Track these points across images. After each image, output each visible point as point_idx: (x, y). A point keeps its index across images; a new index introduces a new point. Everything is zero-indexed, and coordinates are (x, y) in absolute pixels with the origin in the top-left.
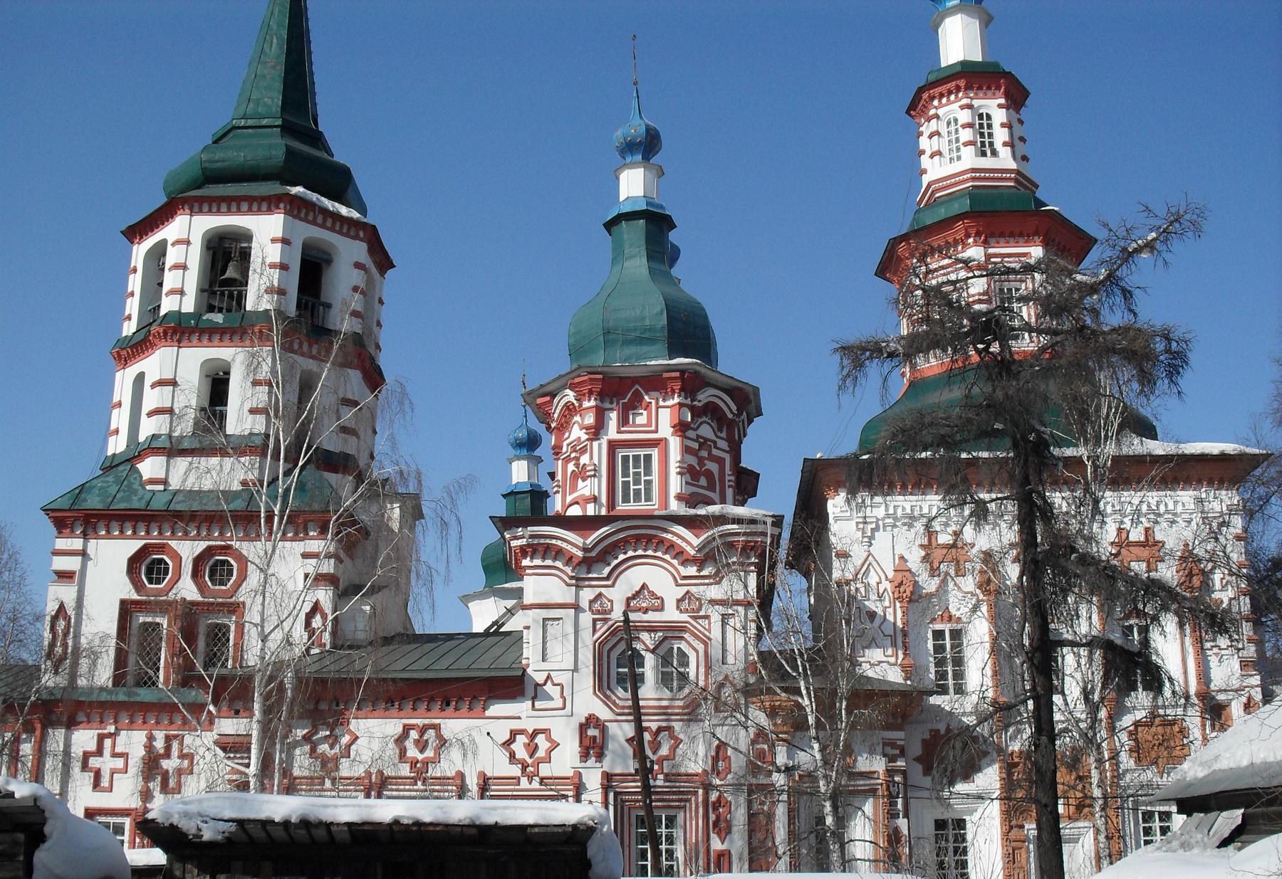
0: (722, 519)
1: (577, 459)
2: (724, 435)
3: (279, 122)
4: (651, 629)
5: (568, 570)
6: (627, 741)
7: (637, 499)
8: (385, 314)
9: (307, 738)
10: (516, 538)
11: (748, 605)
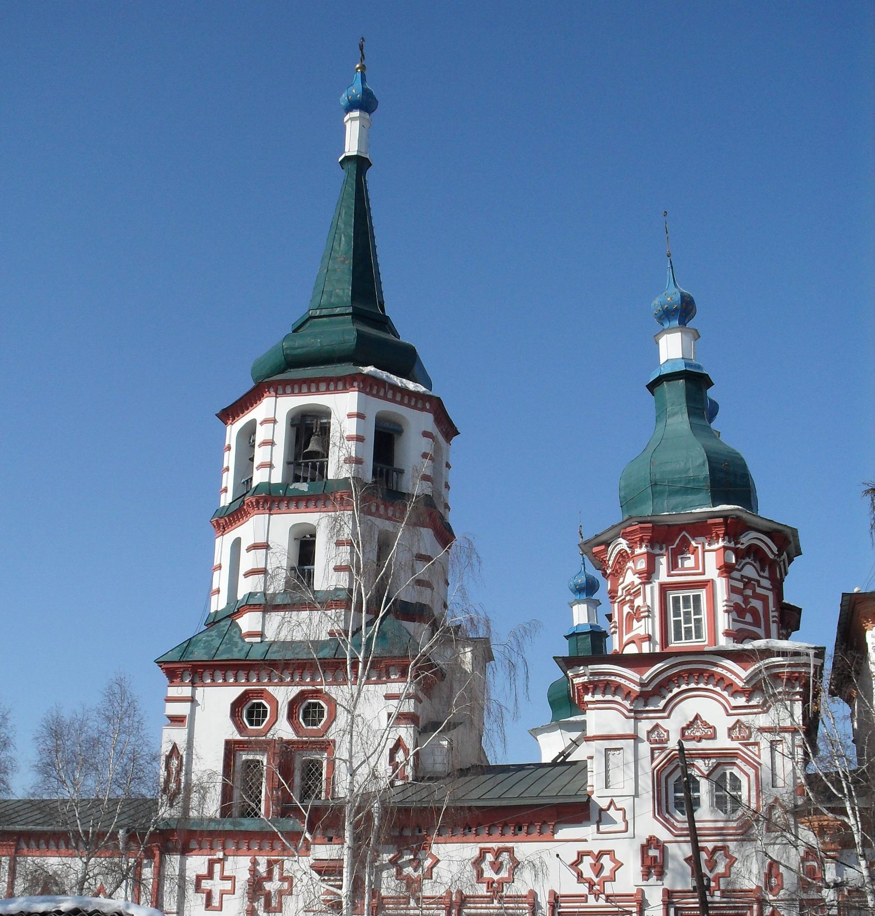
0: (767, 653)
1: (632, 601)
2: (766, 574)
3: (350, 310)
4: (705, 756)
5: (627, 703)
6: (686, 860)
7: (688, 635)
8: (452, 476)
9: (393, 862)
10: (578, 676)
11: (794, 731)
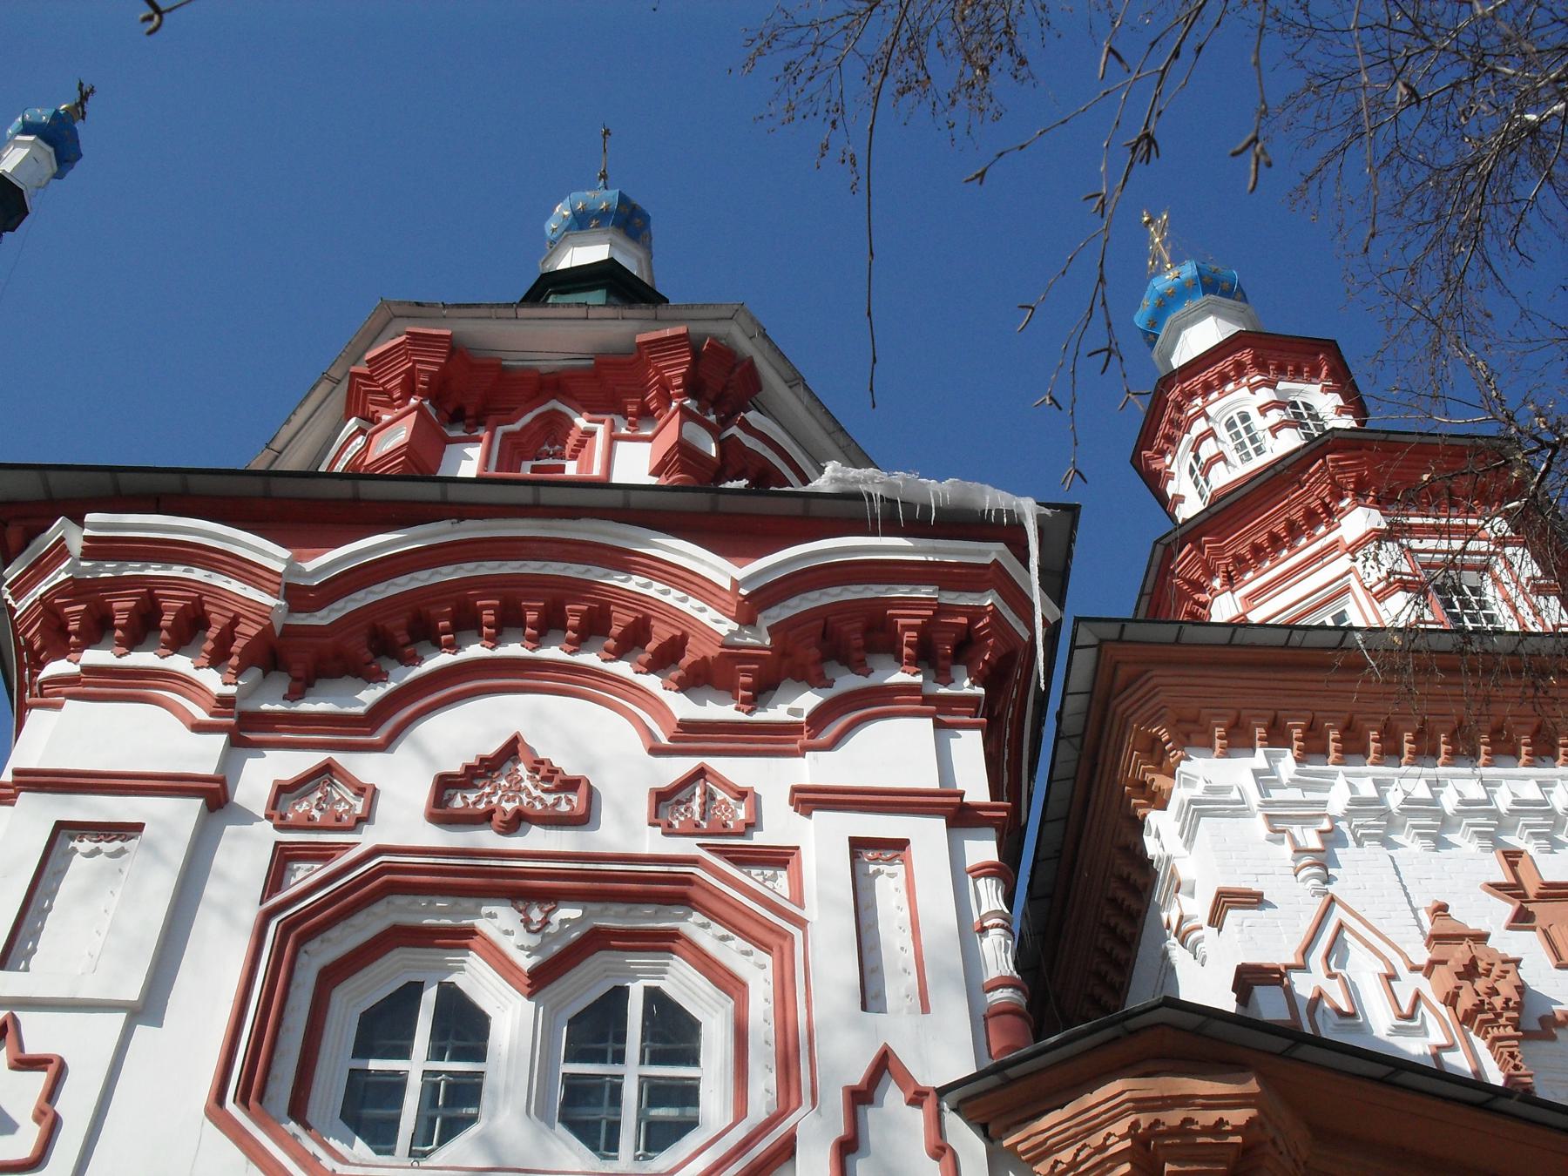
5: (213, 681)
11: (961, 817)
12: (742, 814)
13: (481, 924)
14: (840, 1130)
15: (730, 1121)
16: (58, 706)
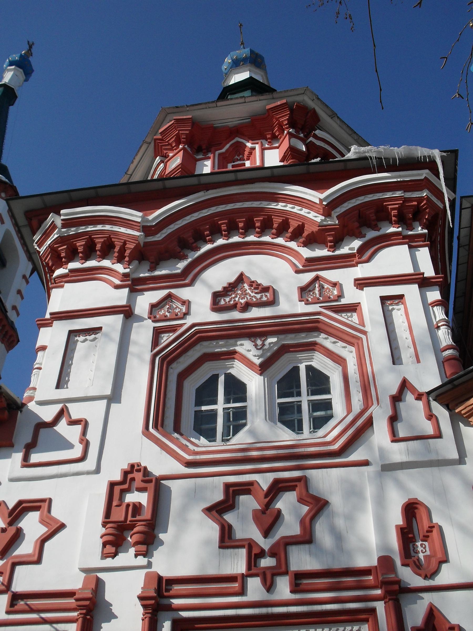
5: (120, 268)
11: (424, 283)
12: (335, 292)
13: (238, 349)
14: (390, 413)
15: (345, 414)
16: (62, 287)
